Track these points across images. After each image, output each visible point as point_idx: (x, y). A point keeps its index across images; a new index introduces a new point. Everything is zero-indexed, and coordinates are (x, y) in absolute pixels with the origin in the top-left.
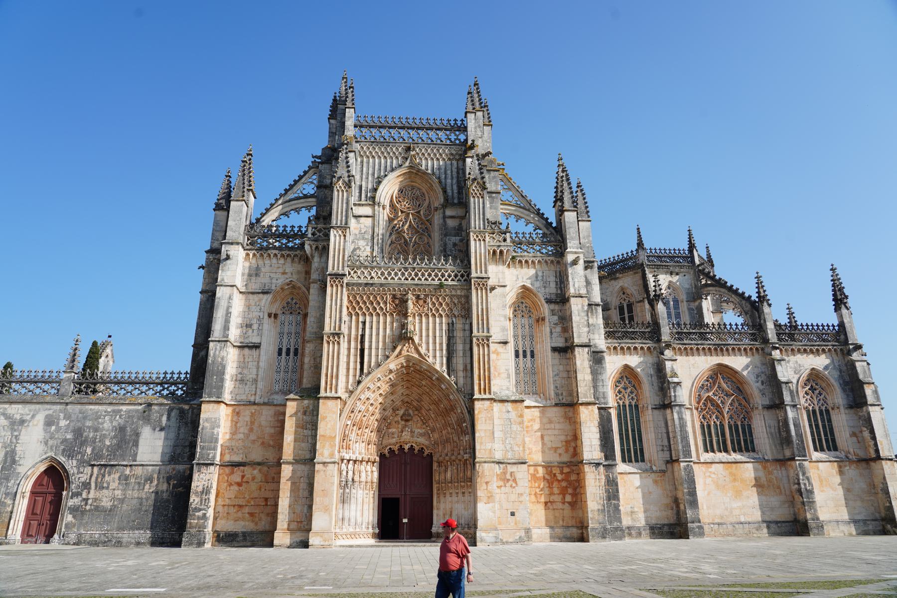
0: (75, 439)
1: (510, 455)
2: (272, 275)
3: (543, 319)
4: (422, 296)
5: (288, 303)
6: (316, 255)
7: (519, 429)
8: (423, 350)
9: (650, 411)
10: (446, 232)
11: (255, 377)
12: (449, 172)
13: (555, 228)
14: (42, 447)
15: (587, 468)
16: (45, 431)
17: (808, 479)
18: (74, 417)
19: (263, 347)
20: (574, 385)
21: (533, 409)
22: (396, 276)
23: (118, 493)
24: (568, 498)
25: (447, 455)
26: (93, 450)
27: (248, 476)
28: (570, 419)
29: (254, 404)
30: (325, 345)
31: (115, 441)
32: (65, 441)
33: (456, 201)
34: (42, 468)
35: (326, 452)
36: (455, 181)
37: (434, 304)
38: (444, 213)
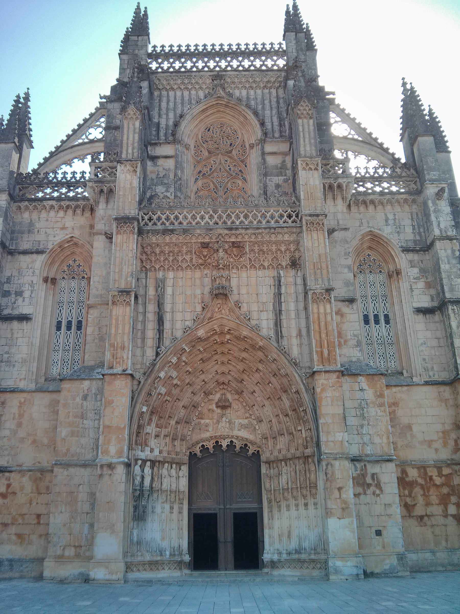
2: (48, 231)
6: (102, 200)
7: (379, 413)
12: (267, 102)
19: (38, 319)
21: (394, 389)
25: (280, 451)
29: (22, 391)
33: (277, 135)
35: (113, 450)
36: (274, 112)
38: (263, 148)
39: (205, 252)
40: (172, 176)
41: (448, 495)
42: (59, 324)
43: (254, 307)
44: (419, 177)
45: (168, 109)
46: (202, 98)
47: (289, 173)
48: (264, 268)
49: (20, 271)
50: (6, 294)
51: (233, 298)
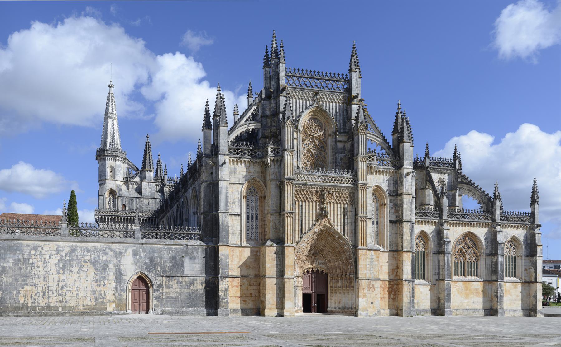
0: (151, 263)
1: (372, 276)
4: (331, 192)
8: (332, 223)
10: (336, 151)
13: (393, 149)
14: (133, 267)
15: (404, 283)
16: (134, 258)
17: (502, 290)
18: (148, 251)
20: (400, 241)
22: (316, 179)
23: (178, 290)
26: (161, 268)
30: (286, 219)
31: (171, 264)
32: (145, 263)
33: (342, 131)
36: (341, 117)
37: (337, 197)
39: (318, 194)
51: (329, 216)
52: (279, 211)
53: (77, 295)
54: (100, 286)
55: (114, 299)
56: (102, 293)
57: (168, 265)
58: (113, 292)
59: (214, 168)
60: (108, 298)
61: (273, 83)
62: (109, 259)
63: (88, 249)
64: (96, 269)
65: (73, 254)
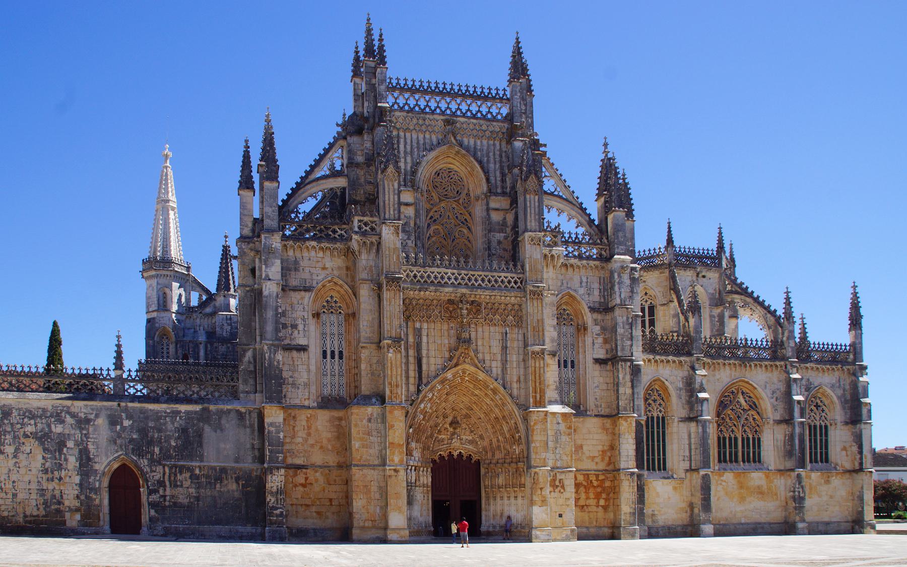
0: (142, 439)
3: (585, 329)
5: (336, 302)
9: (675, 424)
10: (490, 228)
11: (306, 381)
12: (491, 154)
13: (597, 226)
17: (802, 487)
19: (312, 349)
23: (192, 490)
24: (602, 502)
26: (160, 450)
27: (311, 478)
28: (607, 430)
29: (309, 408)
32: (132, 441)
33: (499, 191)
34: (116, 466)
36: (497, 166)
38: (488, 204)
40: (412, 224)
41: (601, 493)
42: (325, 352)
43: (487, 357)
44: (609, 245)
45: (405, 152)
46: (435, 143)
47: (508, 230)
48: (495, 325)
49: (292, 305)
50: (285, 326)
52: (377, 340)
53: (15, 495)
54: (52, 480)
55: (78, 505)
56: (57, 493)
57: (173, 443)
58: (76, 492)
59: (257, 260)
60: (67, 503)
61: (366, 104)
62: (67, 432)
63: (30, 412)
64: (45, 450)
65: (6, 421)
